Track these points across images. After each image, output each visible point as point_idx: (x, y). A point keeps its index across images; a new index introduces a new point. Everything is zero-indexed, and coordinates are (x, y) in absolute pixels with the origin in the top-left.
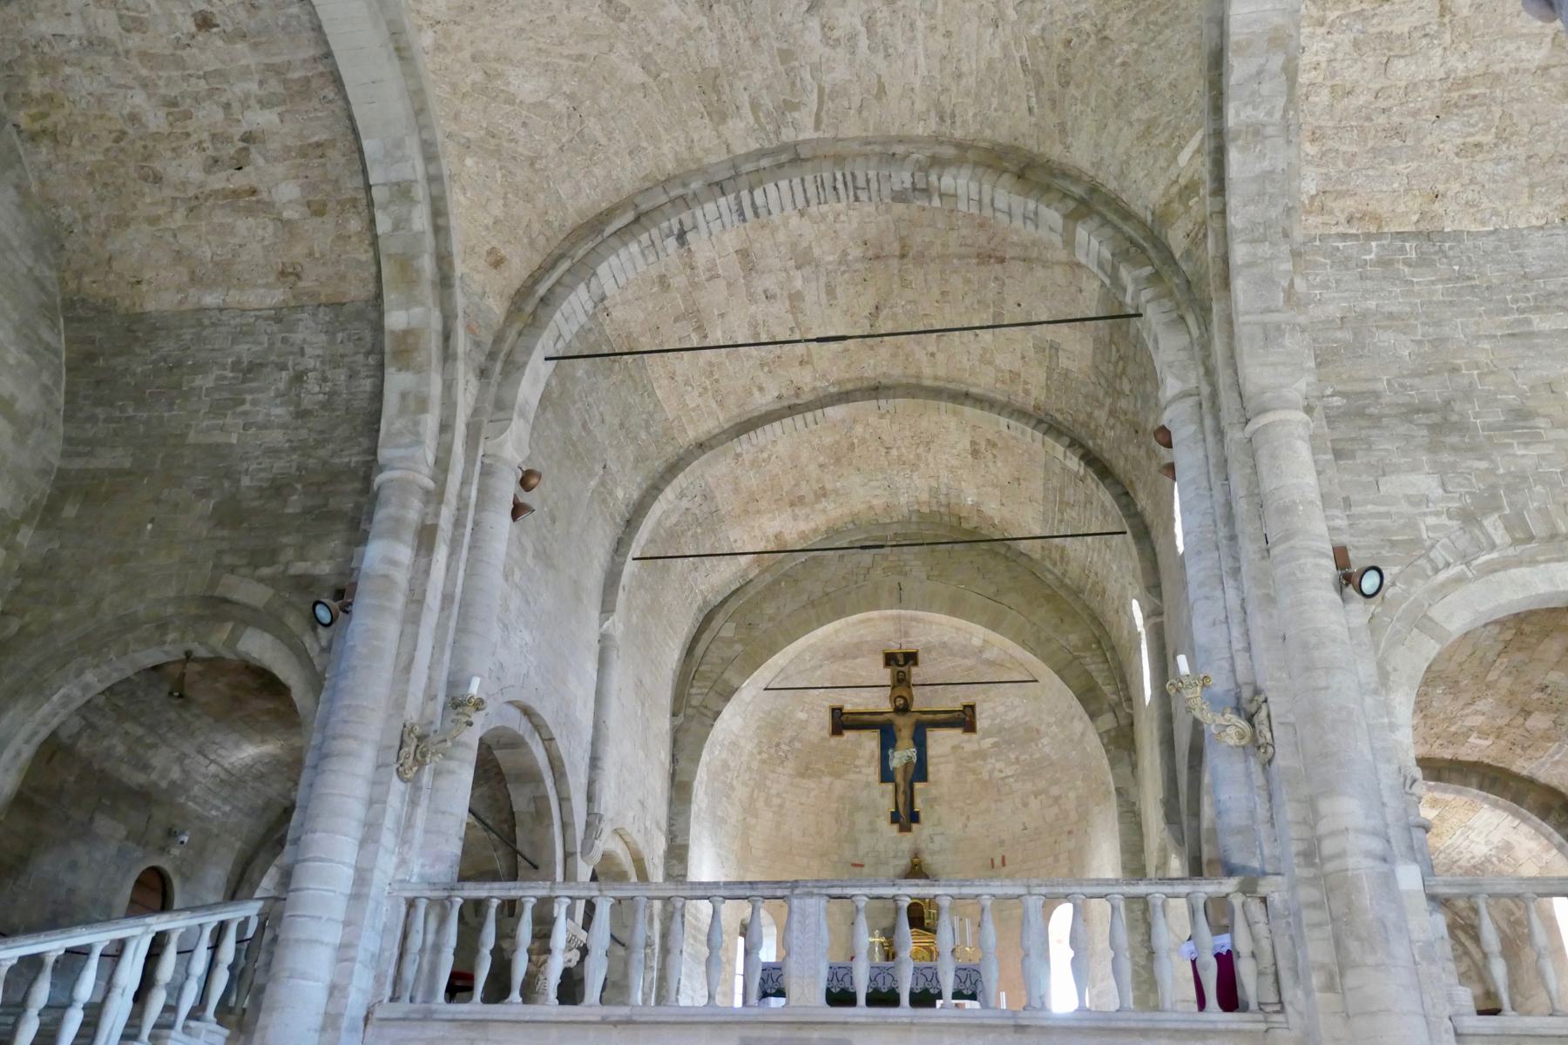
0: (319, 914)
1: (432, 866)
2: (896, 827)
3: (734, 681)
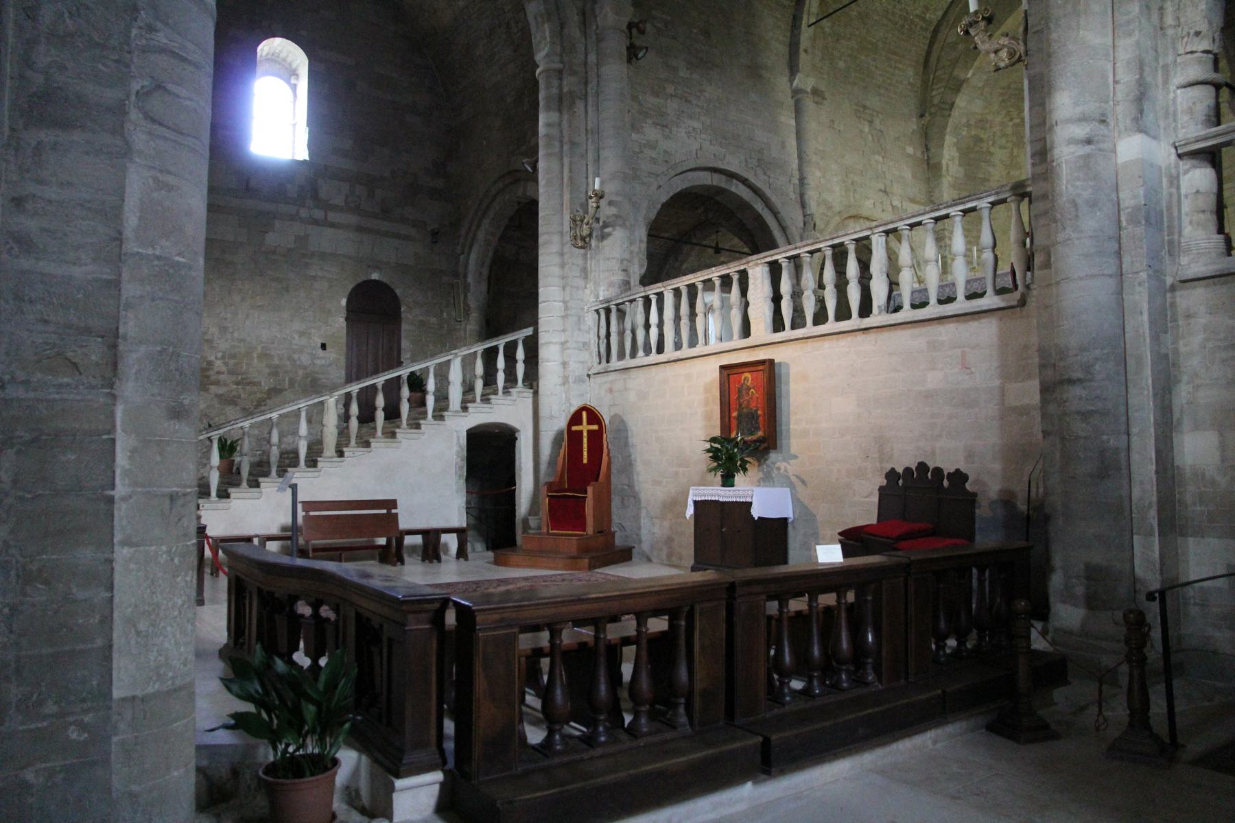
0: (547, 329)
1: (608, 290)
3: (962, 76)
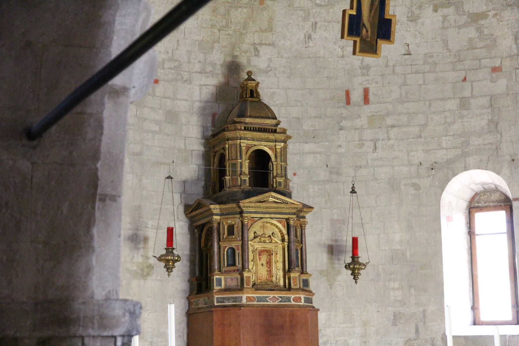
2: (349, 43)
